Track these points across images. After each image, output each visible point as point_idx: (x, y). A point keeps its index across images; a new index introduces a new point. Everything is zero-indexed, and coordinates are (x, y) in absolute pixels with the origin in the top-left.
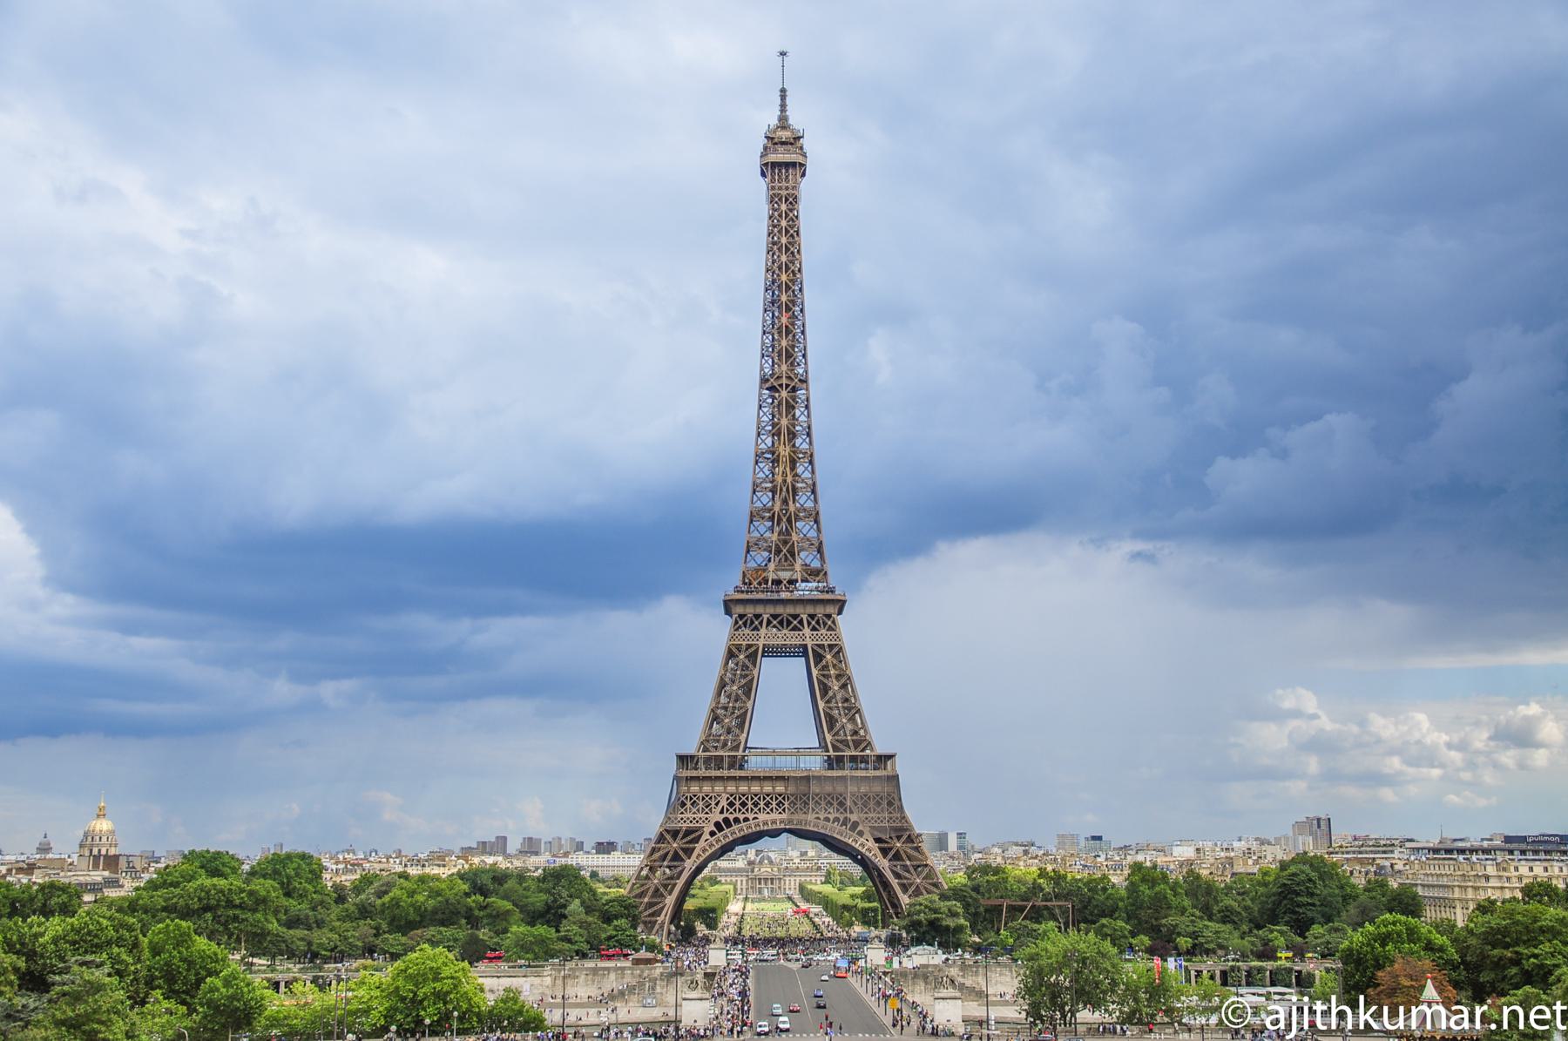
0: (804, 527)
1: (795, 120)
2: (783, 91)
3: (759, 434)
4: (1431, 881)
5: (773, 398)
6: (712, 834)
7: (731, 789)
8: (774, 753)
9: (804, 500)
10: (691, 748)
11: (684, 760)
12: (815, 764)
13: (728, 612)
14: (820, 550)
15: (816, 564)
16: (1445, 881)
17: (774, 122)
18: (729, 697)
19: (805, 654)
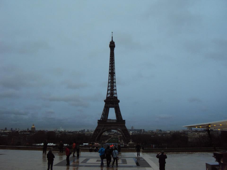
0: (115, 92)
1: (114, 41)
2: (112, 37)
3: (109, 80)
4: (190, 135)
5: (111, 75)
6: (102, 130)
7: (105, 124)
8: (110, 120)
9: (114, 88)
10: (99, 119)
11: (98, 120)
12: (115, 121)
13: (105, 102)
14: (117, 94)
15: (116, 96)
16: (192, 135)
17: (111, 41)
18: (105, 113)
19: (114, 107)
